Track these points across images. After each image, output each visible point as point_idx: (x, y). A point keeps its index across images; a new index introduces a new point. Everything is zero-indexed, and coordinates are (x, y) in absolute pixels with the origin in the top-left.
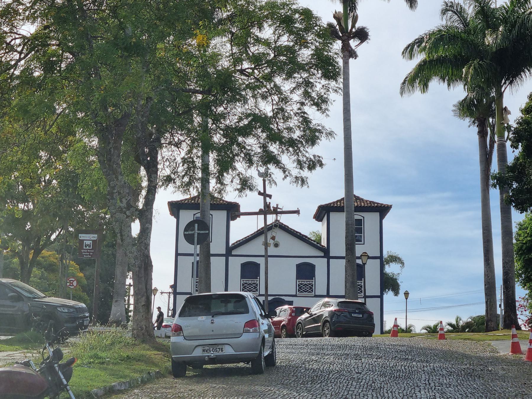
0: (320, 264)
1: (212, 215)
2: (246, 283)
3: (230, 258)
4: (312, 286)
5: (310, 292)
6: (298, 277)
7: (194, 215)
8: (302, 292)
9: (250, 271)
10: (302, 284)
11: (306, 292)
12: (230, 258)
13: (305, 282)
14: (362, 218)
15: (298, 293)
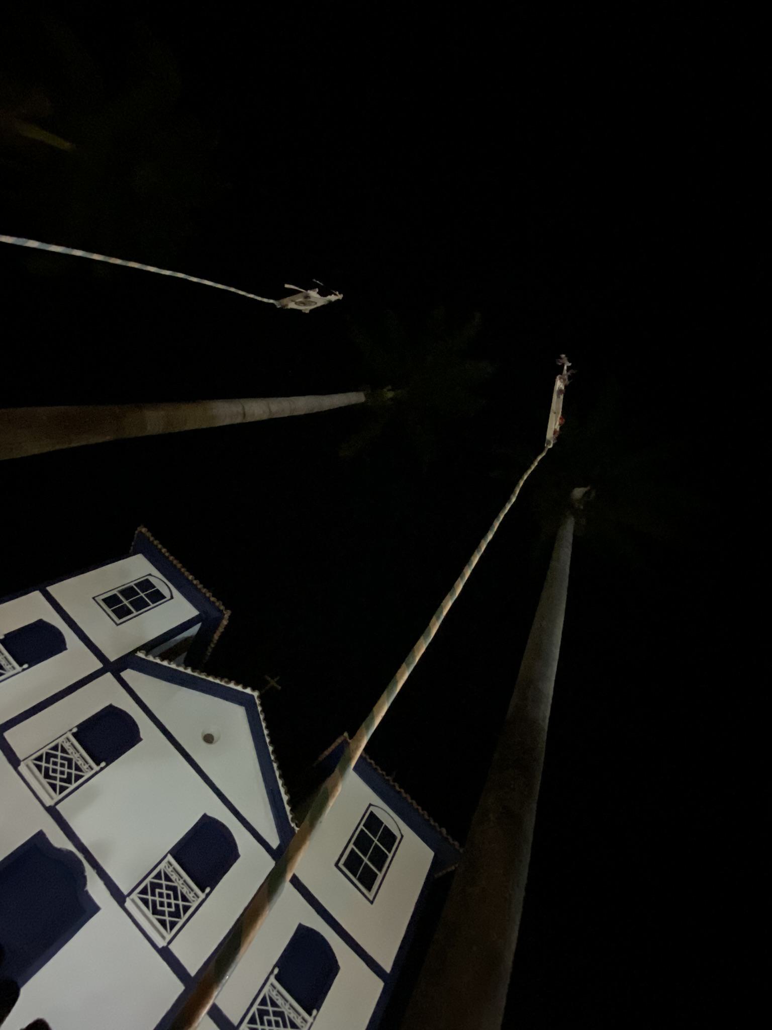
0: (251, 866)
1: (172, 597)
2: (64, 750)
3: (109, 675)
4: (186, 909)
5: (163, 923)
6: (181, 852)
7: (150, 575)
8: (146, 902)
9: (108, 737)
10: (168, 878)
11: (155, 912)
12: (109, 675)
13: (182, 880)
14: (399, 837)
15: (135, 896)
